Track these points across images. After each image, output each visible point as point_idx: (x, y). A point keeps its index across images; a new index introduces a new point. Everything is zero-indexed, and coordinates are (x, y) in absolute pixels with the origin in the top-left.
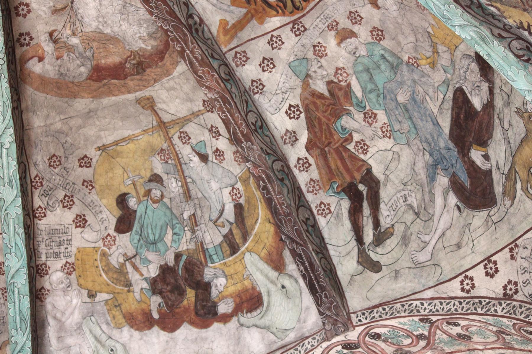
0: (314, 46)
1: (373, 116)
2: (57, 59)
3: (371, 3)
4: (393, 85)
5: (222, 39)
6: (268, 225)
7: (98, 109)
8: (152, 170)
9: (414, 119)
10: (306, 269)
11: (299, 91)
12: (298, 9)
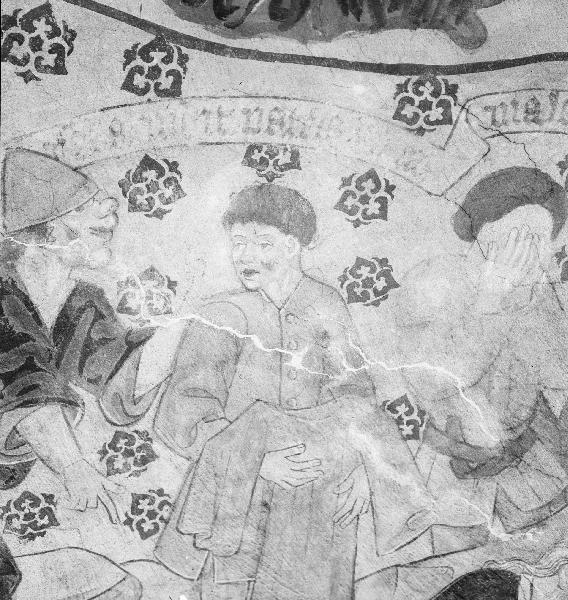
0: (148, 163)
1: (138, 455)
3: (462, 208)
9: (273, 540)
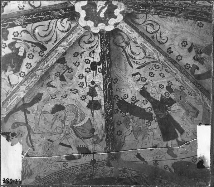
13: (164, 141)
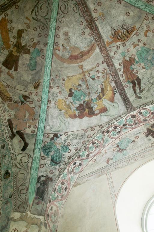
2: (63, 51)
4: (147, 56)
5: (107, 45)
6: (111, 91)
7: (69, 67)
8: (79, 83)
10: (124, 96)
11: (122, 59)
12: (125, 40)
13: (2, 64)
